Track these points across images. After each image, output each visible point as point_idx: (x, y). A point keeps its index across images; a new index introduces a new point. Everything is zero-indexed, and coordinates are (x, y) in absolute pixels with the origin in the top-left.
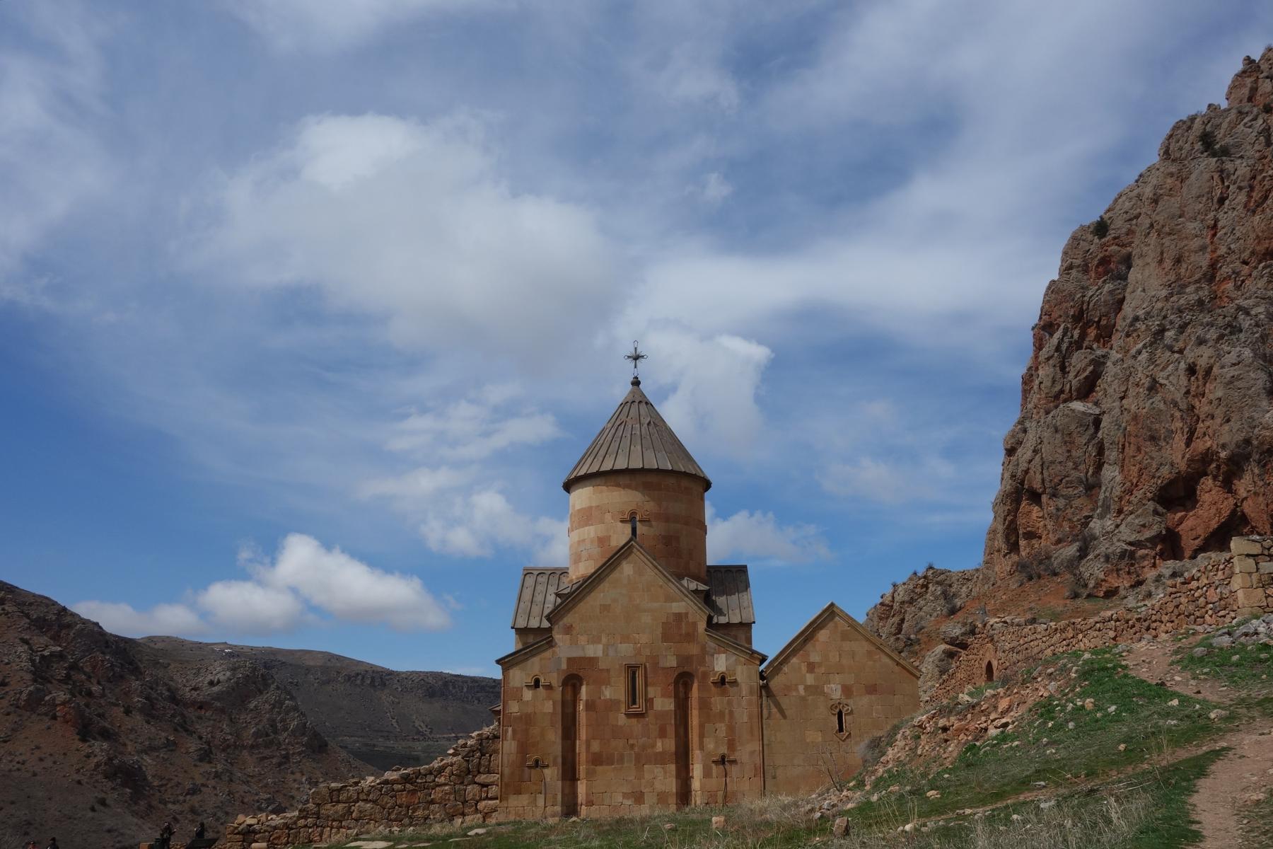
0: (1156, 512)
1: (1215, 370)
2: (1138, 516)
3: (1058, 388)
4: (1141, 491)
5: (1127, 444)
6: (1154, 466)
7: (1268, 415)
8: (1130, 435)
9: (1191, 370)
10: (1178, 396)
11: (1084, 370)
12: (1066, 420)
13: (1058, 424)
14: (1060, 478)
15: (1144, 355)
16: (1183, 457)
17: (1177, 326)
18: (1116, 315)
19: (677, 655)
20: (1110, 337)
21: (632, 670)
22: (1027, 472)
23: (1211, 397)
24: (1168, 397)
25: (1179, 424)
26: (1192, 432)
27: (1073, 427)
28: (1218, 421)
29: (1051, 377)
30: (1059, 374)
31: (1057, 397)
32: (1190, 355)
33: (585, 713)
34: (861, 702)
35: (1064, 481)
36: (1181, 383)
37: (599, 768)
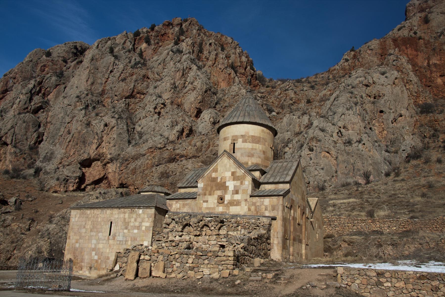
0: (80, 168)
1: (115, 128)
2: (72, 168)
3: (26, 106)
4: (73, 159)
5: (72, 140)
6: (82, 151)
7: (128, 149)
8: (74, 138)
9: (106, 125)
10: (99, 132)
11: (38, 104)
12: (30, 120)
13: (26, 120)
14: (19, 141)
15: (83, 112)
16: (94, 152)
17: (92, 106)
18: (54, 89)
19: (303, 206)
20: (48, 96)
21: (299, 207)
22: (7, 133)
23: (111, 136)
24: (95, 131)
25: (96, 141)
26: (99, 145)
27: (31, 124)
28: (112, 145)
29: (26, 101)
30: (28, 102)
31: (24, 109)
32: (107, 119)
33: (293, 221)
34: (319, 230)
35: (20, 142)
36: (101, 127)
37: (295, 242)
